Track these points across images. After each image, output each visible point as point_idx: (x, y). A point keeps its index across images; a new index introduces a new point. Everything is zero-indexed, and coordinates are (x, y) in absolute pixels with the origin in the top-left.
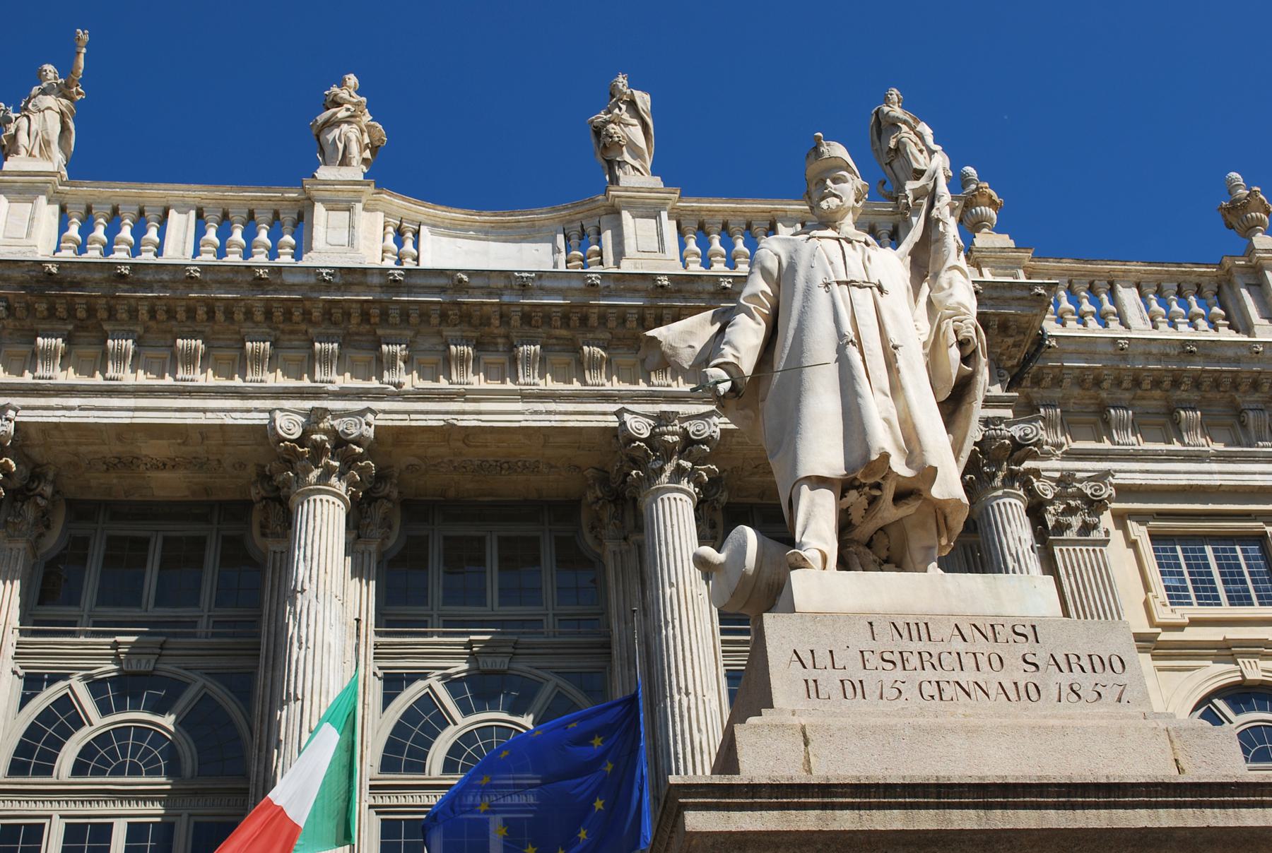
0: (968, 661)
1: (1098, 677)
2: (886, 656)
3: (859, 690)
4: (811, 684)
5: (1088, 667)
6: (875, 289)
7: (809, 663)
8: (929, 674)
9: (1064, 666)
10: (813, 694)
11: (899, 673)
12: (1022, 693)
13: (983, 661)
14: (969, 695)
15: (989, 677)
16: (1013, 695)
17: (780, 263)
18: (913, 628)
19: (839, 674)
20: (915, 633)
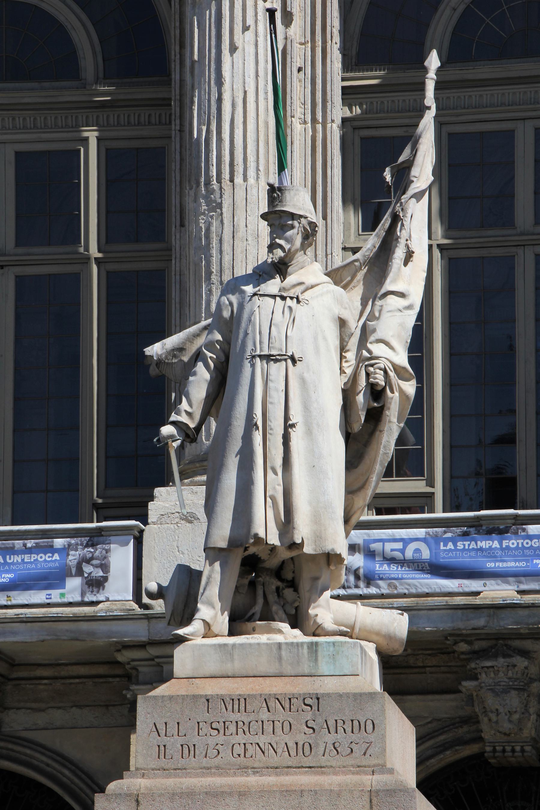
0: (268, 728)
1: (354, 737)
2: (214, 726)
3: (192, 752)
4: (162, 748)
5: (349, 730)
6: (289, 361)
7: (162, 733)
8: (241, 738)
9: (332, 730)
10: (162, 756)
11: (221, 738)
12: (300, 750)
13: (278, 725)
14: (263, 752)
15: (282, 738)
16: (293, 753)
17: (232, 311)
18: (236, 702)
19: (181, 740)
20: (236, 707)
